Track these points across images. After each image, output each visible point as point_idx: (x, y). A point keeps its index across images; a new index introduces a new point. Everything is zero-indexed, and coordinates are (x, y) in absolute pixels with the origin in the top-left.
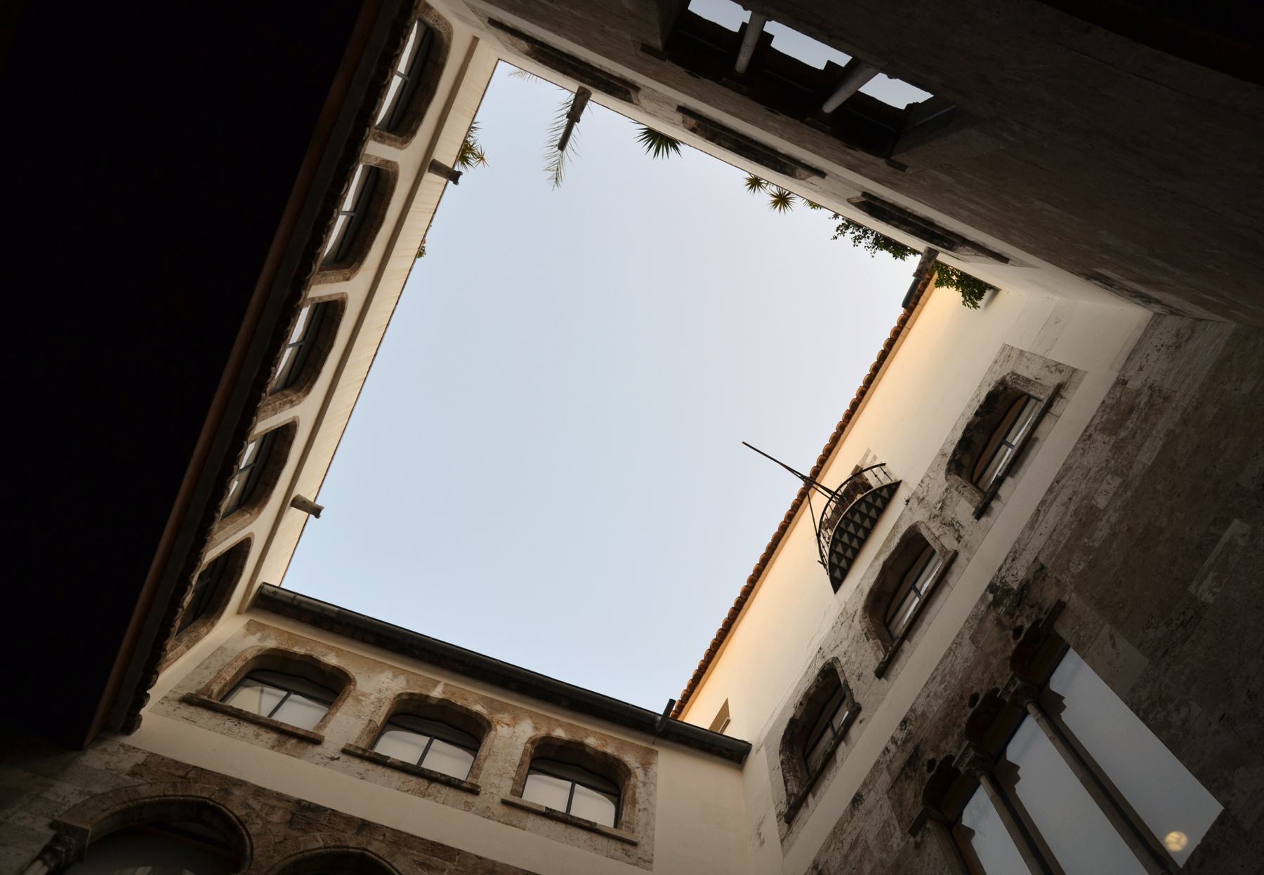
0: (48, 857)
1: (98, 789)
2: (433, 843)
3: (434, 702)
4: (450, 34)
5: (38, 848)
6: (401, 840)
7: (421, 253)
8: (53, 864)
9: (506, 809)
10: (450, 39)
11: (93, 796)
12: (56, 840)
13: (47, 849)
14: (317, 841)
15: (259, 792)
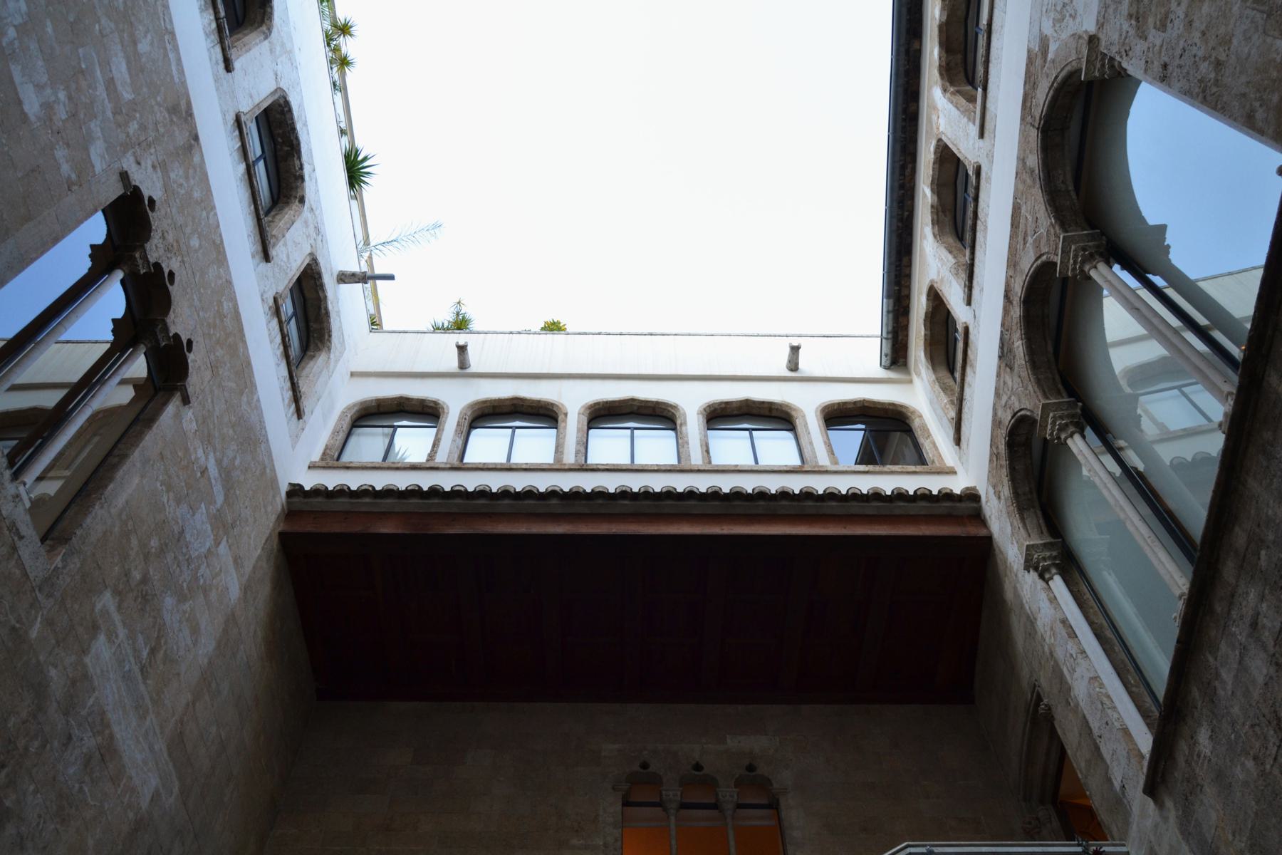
0: (1047, 576)
1: (1009, 529)
2: (1012, 225)
3: (936, 198)
4: (349, 408)
5: (1040, 583)
6: (1013, 262)
7: (553, 327)
8: (1054, 571)
9: (986, 135)
10: (355, 405)
11: (1013, 534)
12: (1036, 569)
13: (1041, 576)
14: (1019, 346)
15: (998, 394)
